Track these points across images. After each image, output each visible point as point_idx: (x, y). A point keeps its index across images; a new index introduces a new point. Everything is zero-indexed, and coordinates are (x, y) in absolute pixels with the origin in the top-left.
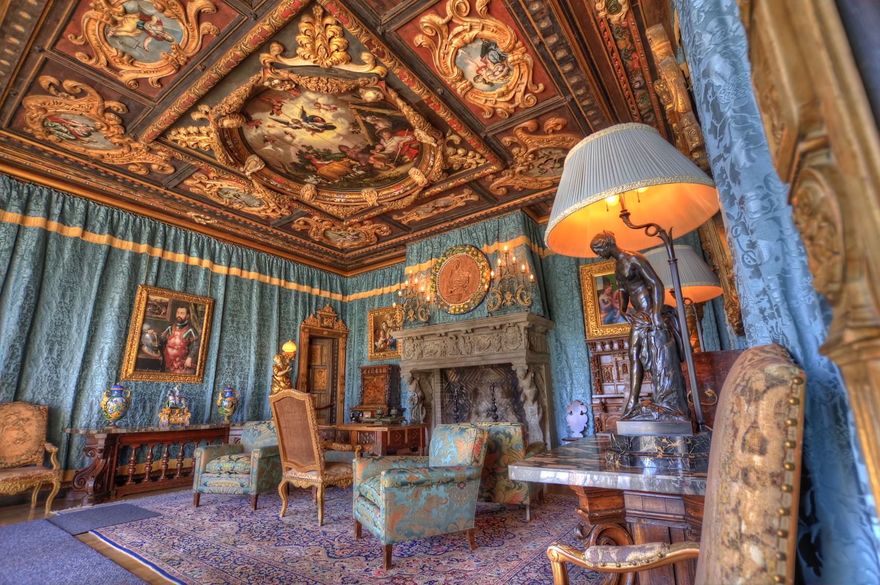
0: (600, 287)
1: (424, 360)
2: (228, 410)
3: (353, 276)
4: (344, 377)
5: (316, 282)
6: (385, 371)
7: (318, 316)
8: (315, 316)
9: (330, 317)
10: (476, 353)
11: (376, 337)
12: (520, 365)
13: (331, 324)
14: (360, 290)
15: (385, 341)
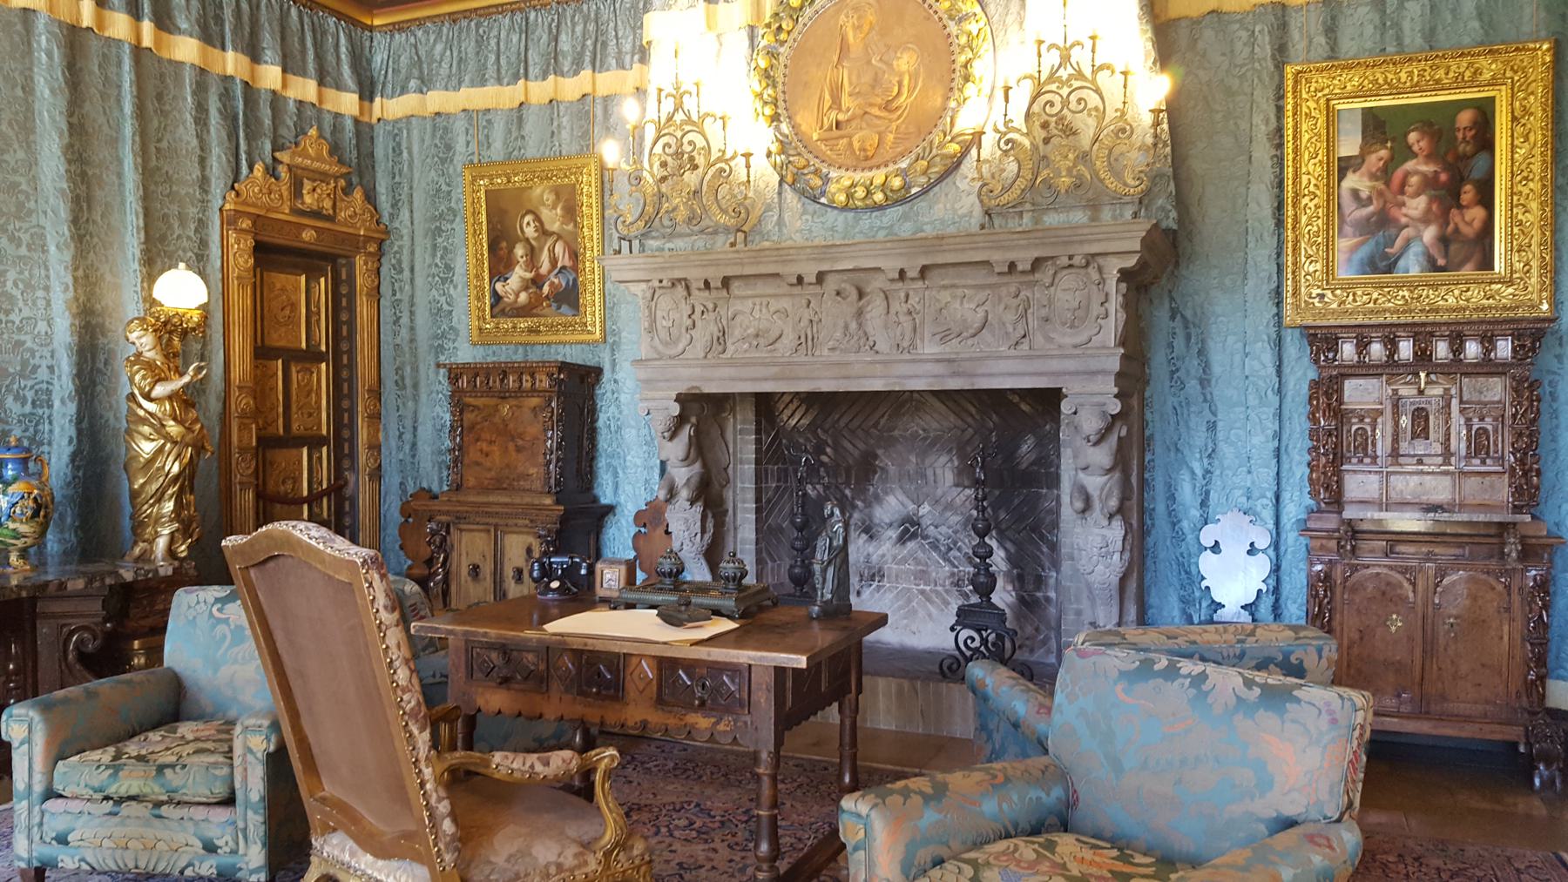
0: (1349, 146)
1: (732, 363)
2: (24, 528)
3: (398, 27)
4: (376, 393)
5: (268, 40)
6: (544, 382)
7: (283, 171)
8: (271, 171)
9: (323, 177)
10: (930, 348)
11: (500, 266)
12: (1090, 398)
13: (327, 204)
14: (425, 84)
15: (537, 282)
